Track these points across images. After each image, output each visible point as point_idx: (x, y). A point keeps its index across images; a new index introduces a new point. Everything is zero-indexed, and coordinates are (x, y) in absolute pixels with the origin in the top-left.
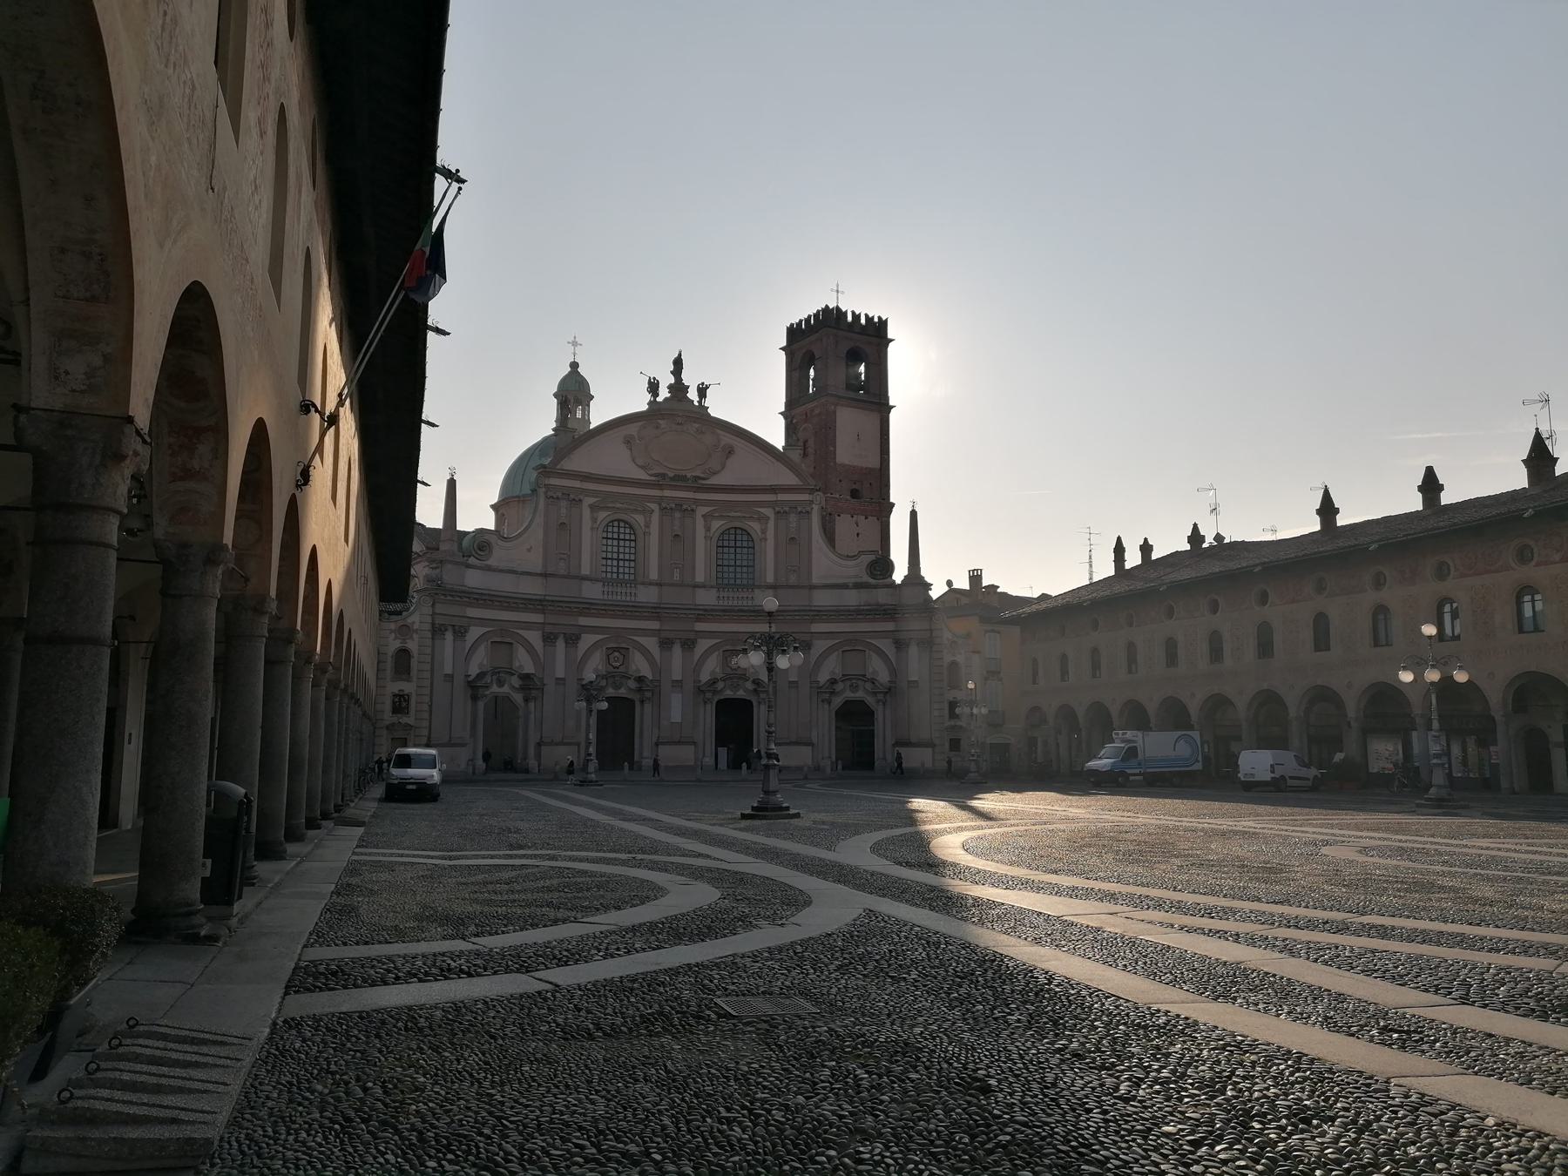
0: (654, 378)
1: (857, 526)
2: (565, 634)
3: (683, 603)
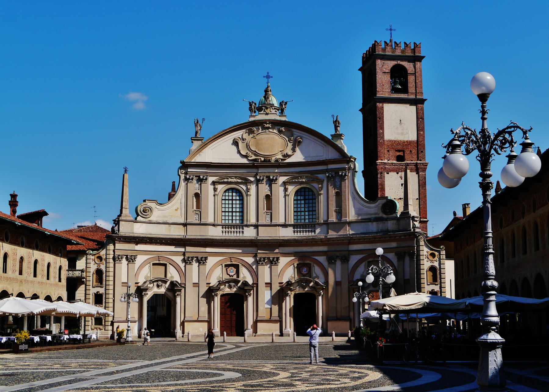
0: (252, 102)
1: (402, 179)
2: (197, 257)
3: (272, 236)
